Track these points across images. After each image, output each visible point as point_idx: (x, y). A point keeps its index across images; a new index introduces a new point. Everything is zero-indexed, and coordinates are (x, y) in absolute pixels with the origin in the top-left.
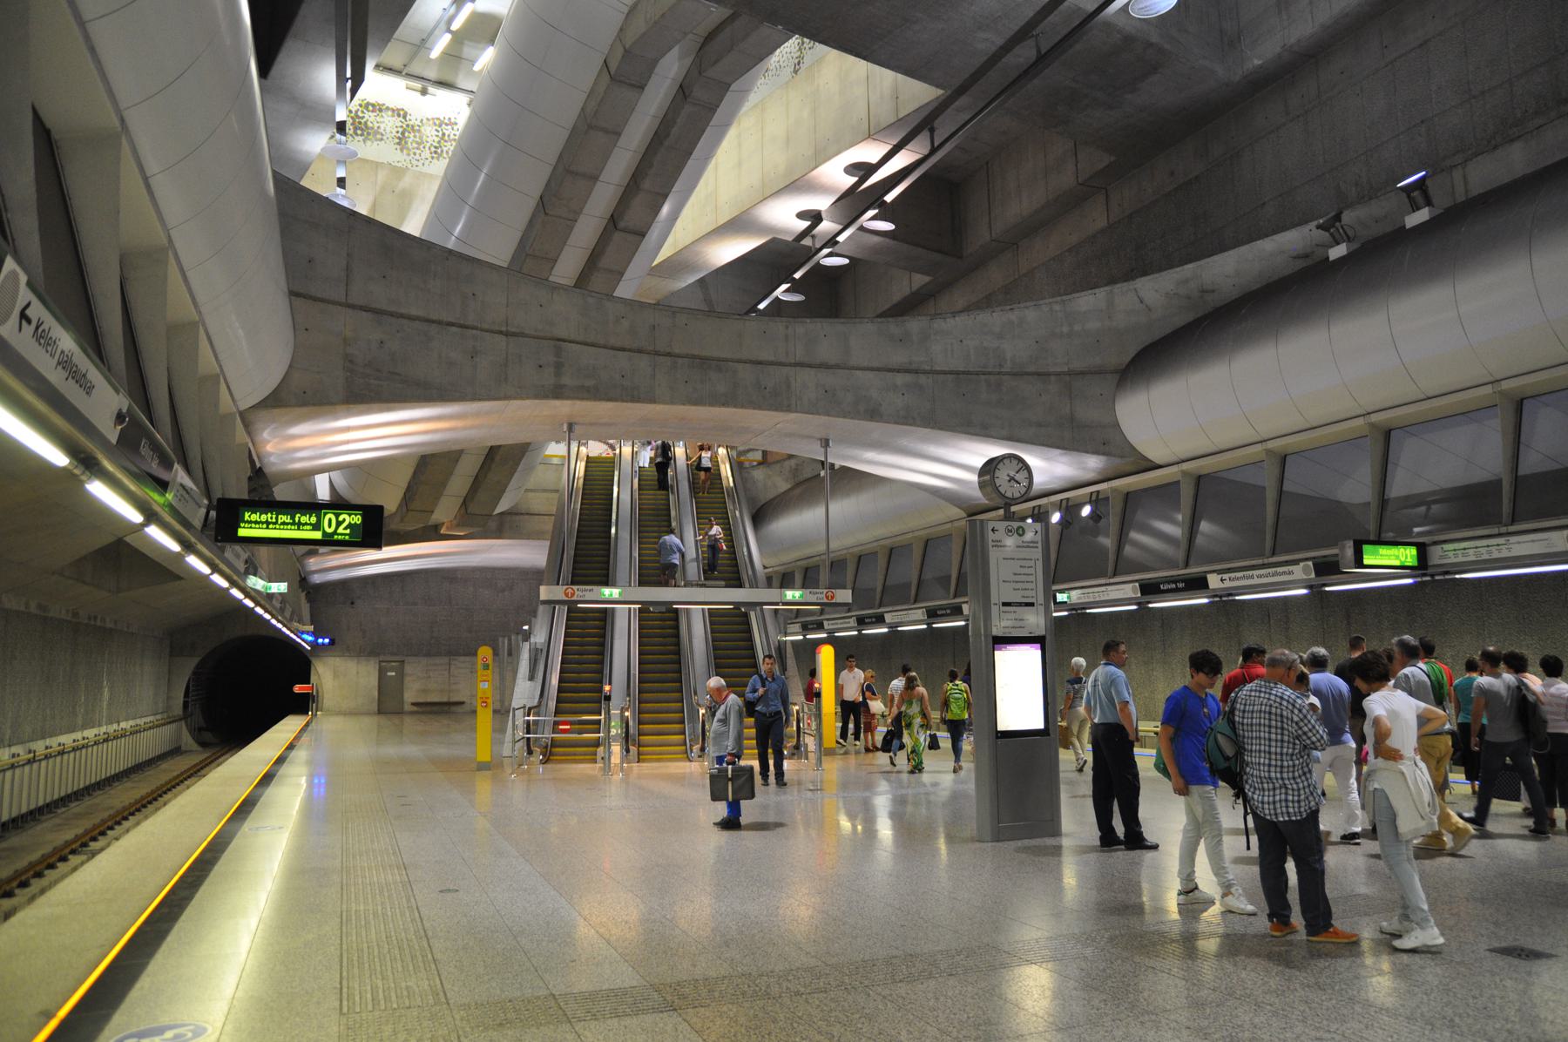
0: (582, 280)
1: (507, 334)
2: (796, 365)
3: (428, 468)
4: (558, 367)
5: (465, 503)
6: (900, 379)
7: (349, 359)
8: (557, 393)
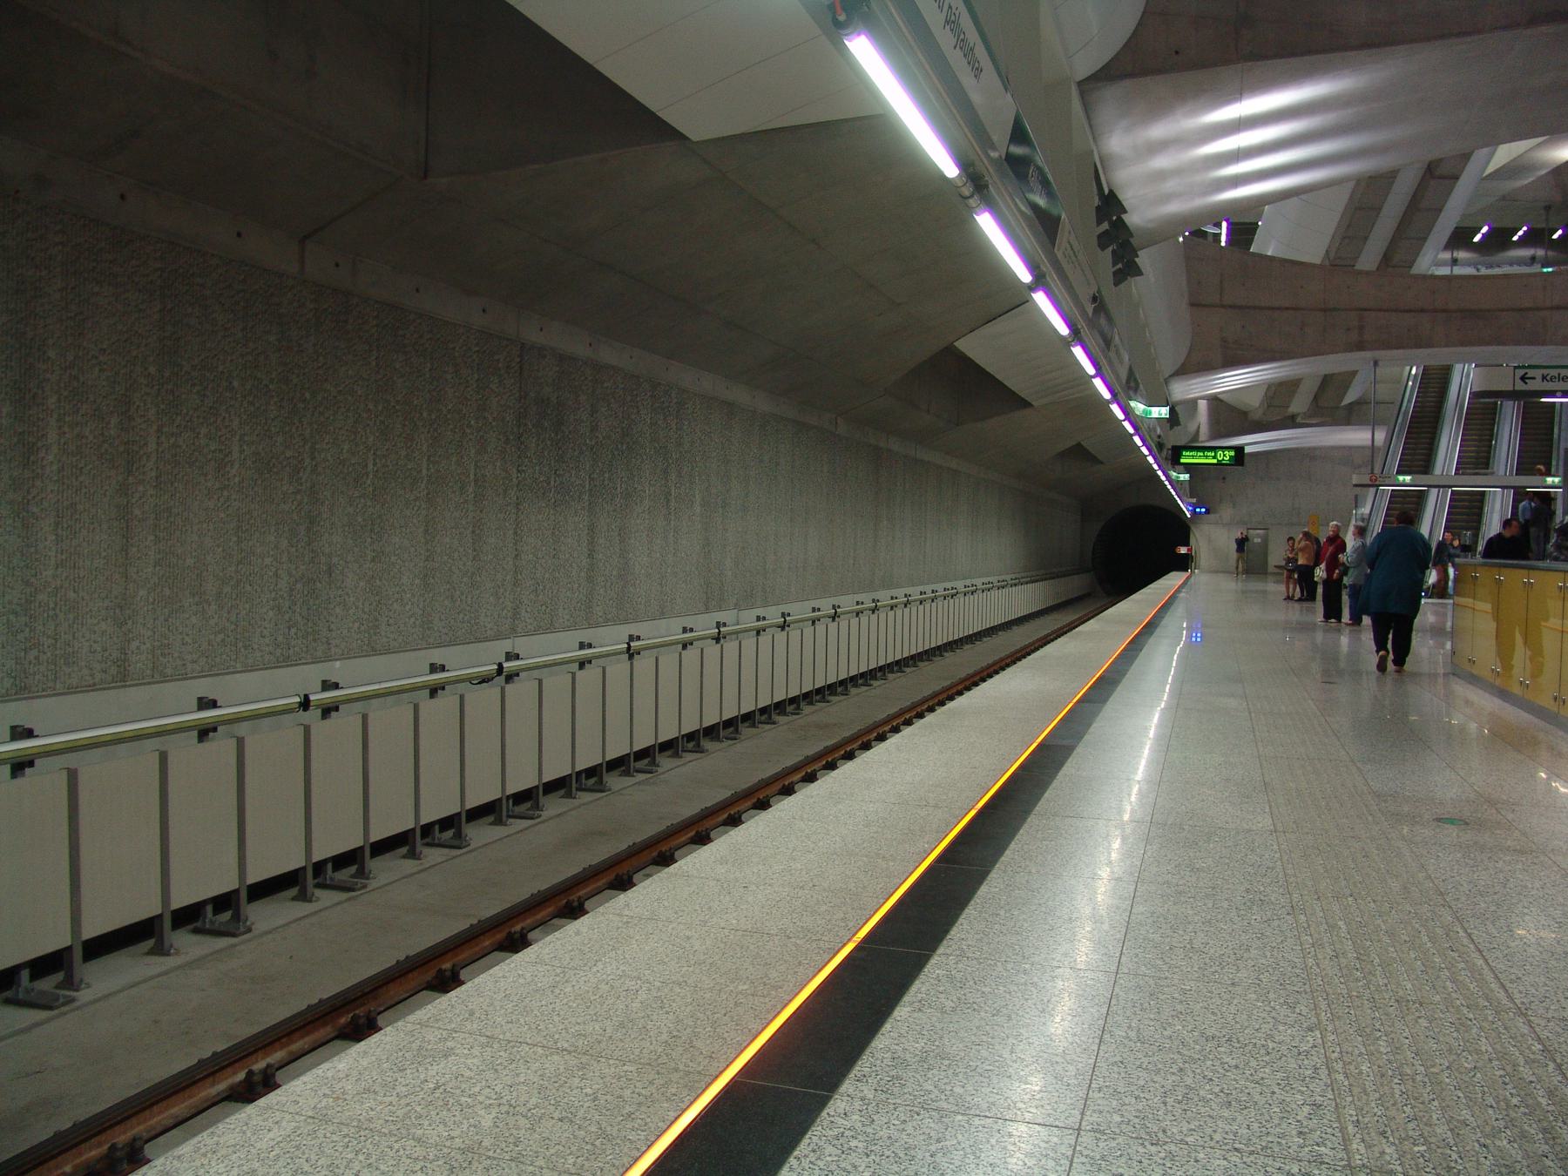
0: (1386, 259)
1: (1325, 310)
2: (1552, 308)
3: (1279, 392)
4: (1361, 328)
5: (1316, 398)
7: (1224, 340)
8: (1360, 346)
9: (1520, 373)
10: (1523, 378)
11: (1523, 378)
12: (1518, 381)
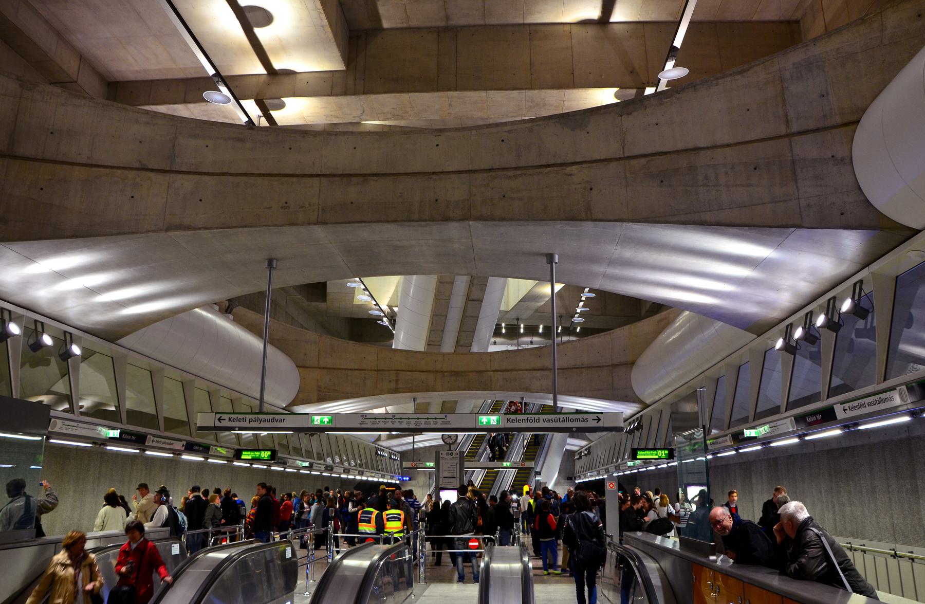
4: (397, 381)
6: (539, 374)
7: (319, 387)
9: (218, 416)
10: (219, 420)
11: (219, 420)
12: (217, 421)
